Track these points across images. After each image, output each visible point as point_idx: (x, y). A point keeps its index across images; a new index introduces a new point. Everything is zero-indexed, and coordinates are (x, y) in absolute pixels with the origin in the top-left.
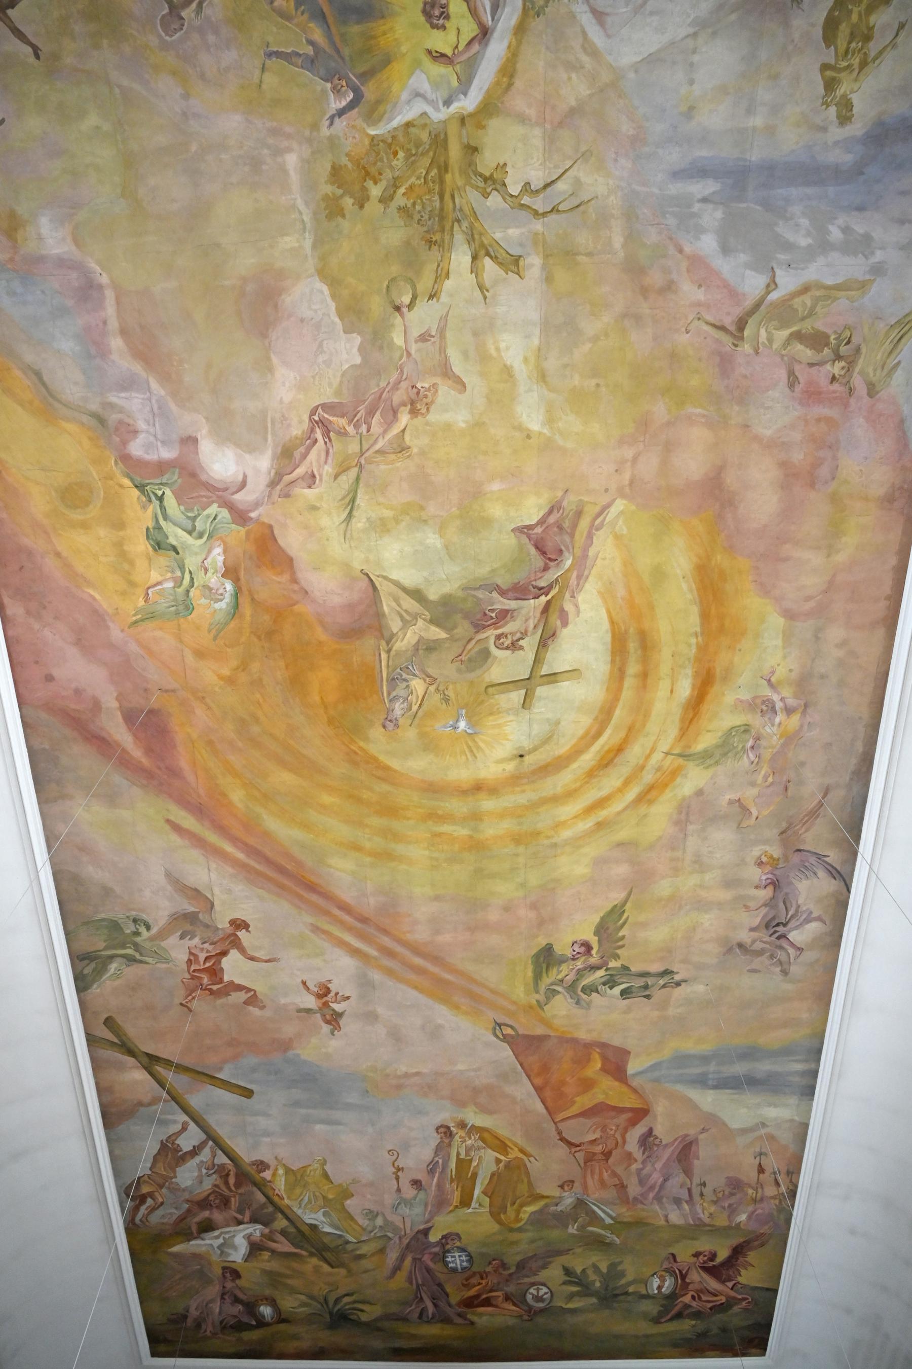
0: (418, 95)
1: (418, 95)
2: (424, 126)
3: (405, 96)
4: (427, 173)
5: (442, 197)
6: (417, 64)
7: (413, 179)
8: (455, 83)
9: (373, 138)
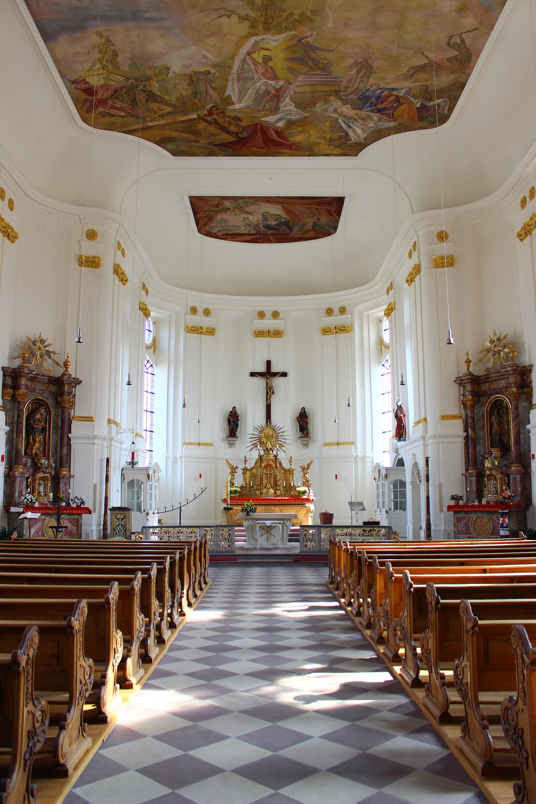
0: (275, 41)
1: (275, 41)
2: (273, 33)
3: (281, 41)
4: (273, 21)
5: (266, 15)
6: (275, 48)
7: (279, 20)
8: (260, 44)
9: (295, 31)
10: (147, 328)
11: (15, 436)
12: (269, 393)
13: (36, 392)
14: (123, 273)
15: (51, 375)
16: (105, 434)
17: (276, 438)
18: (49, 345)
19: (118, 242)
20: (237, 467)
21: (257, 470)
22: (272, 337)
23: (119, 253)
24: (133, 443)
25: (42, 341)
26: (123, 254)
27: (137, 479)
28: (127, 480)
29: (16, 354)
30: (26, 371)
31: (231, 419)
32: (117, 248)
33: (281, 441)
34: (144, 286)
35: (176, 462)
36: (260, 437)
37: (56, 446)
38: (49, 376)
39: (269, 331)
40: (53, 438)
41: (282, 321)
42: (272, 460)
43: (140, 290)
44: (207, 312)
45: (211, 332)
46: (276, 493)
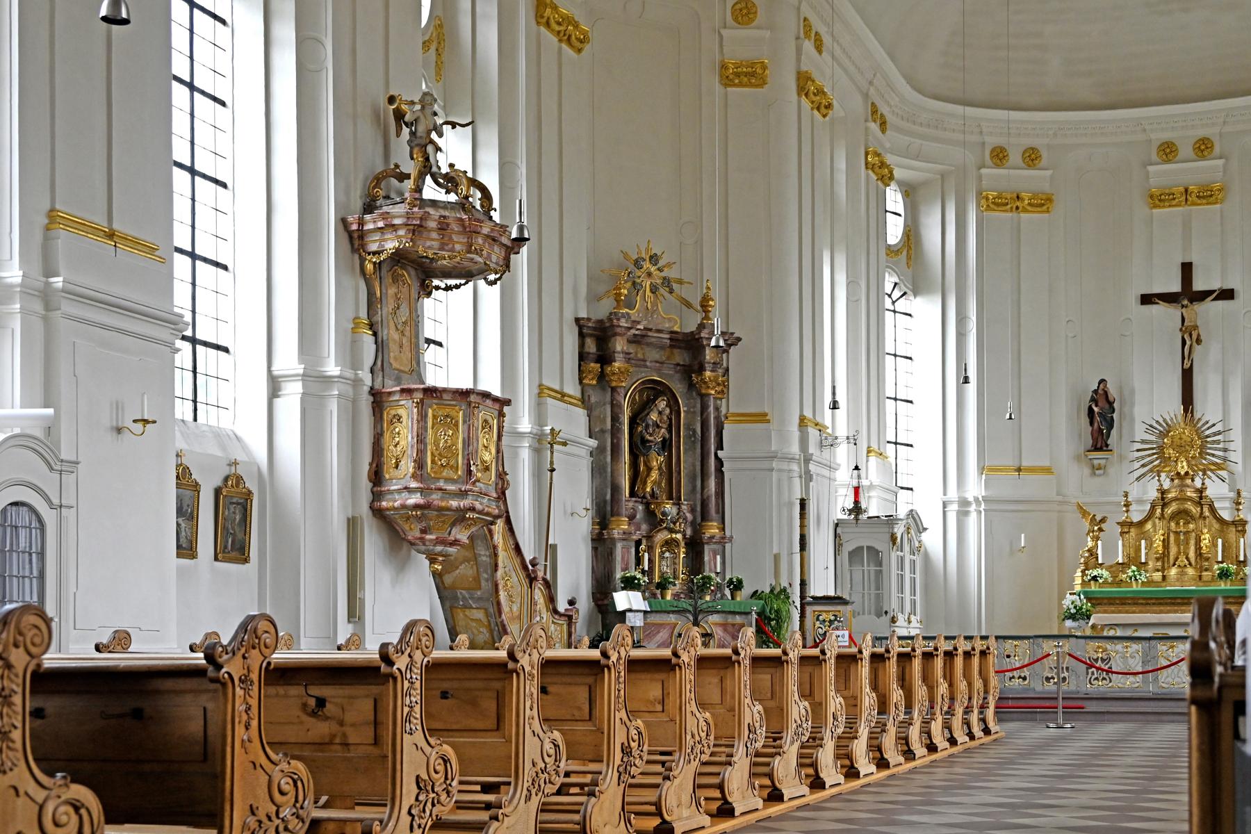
10: (890, 206)
11: (609, 459)
12: (1188, 343)
13: (646, 367)
14: (820, 92)
15: (676, 329)
16: (795, 449)
17: (1202, 447)
18: (669, 265)
19: (805, 19)
20: (1103, 520)
21: (1154, 526)
22: (1194, 204)
23: (808, 46)
24: (857, 468)
25: (654, 259)
26: (819, 47)
27: (872, 542)
28: (848, 548)
29: (602, 289)
30: (623, 323)
31: (1096, 409)
32: (802, 35)
33: (1213, 455)
34: (875, 111)
35: (967, 513)
36: (1161, 448)
37: (692, 478)
38: (672, 332)
39: (1186, 190)
40: (687, 461)
41: (1220, 162)
42: (1190, 499)
43: (866, 121)
44: (1032, 157)
45: (1043, 203)
46: (1200, 577)
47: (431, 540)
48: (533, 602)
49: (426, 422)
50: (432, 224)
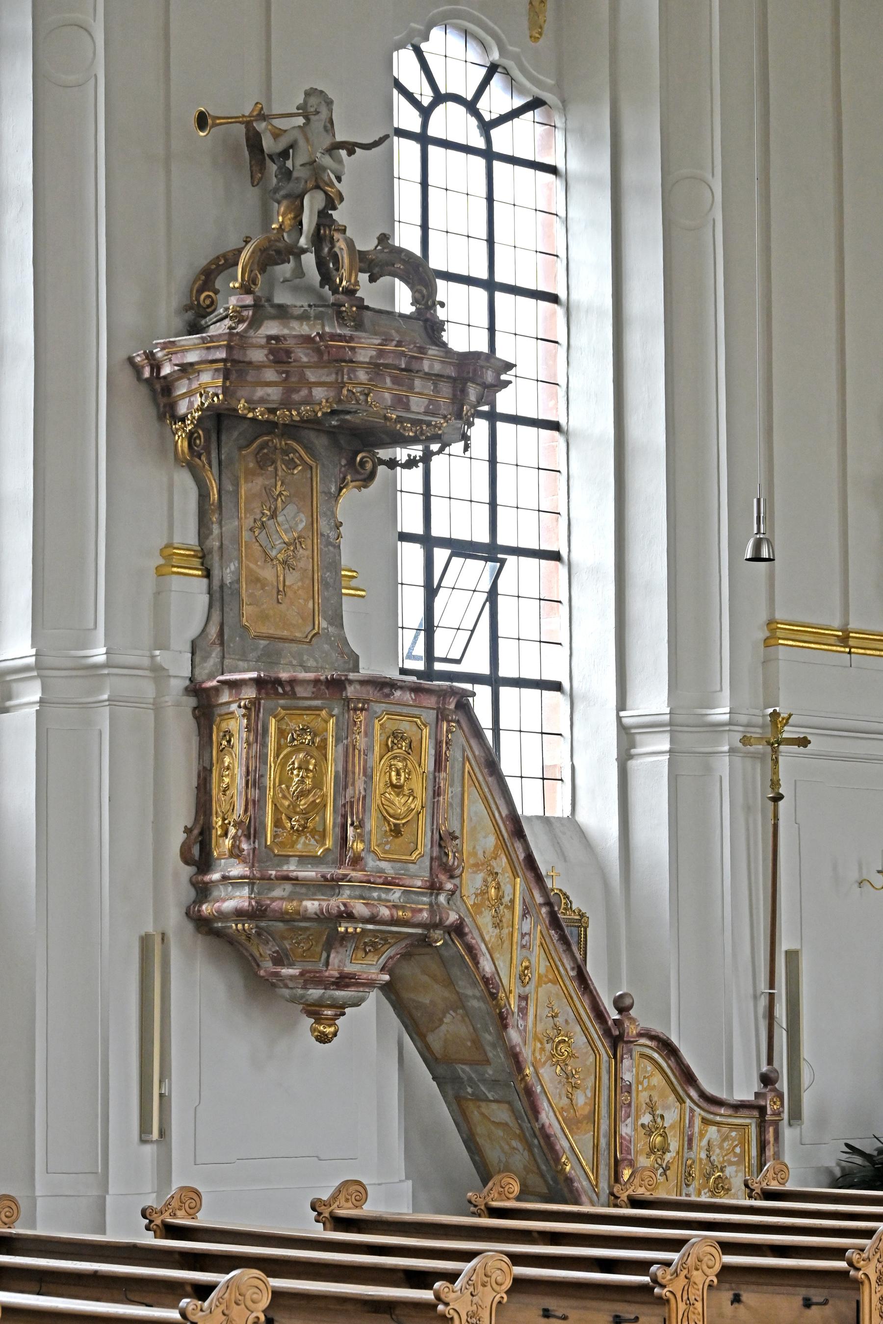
47: (292, 978)
48: (620, 1087)
49: (264, 745)
50: (258, 356)
